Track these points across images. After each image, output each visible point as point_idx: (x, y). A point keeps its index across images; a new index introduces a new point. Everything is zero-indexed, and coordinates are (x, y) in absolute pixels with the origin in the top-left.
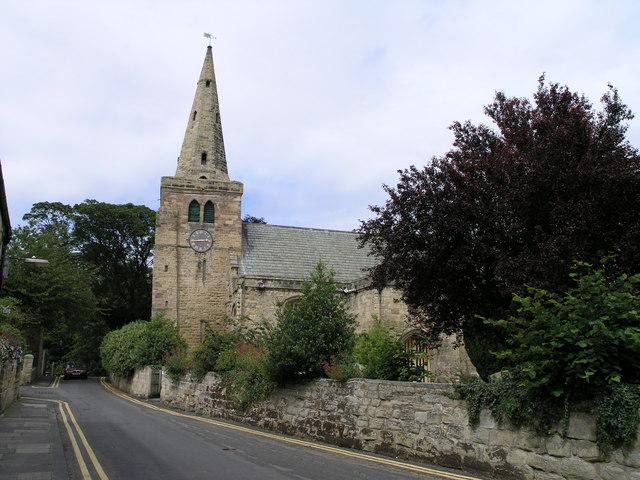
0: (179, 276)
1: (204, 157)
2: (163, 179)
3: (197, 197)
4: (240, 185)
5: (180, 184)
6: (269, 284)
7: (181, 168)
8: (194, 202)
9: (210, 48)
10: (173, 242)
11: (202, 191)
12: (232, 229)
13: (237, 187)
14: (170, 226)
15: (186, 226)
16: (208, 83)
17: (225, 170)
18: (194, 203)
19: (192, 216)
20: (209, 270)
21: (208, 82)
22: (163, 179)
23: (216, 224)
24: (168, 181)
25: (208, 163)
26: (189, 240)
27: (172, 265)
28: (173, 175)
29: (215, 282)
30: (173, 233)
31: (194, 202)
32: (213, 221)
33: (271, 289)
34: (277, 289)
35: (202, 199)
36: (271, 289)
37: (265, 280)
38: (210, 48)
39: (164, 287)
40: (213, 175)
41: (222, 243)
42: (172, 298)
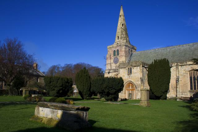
3: (115, 49)
6: (111, 71)
8: (114, 50)
10: (110, 62)
18: (115, 51)
19: (114, 55)
30: (110, 60)
31: (114, 50)
32: (119, 55)
33: (111, 72)
34: (113, 72)
35: (116, 49)
36: (111, 72)
37: (110, 70)
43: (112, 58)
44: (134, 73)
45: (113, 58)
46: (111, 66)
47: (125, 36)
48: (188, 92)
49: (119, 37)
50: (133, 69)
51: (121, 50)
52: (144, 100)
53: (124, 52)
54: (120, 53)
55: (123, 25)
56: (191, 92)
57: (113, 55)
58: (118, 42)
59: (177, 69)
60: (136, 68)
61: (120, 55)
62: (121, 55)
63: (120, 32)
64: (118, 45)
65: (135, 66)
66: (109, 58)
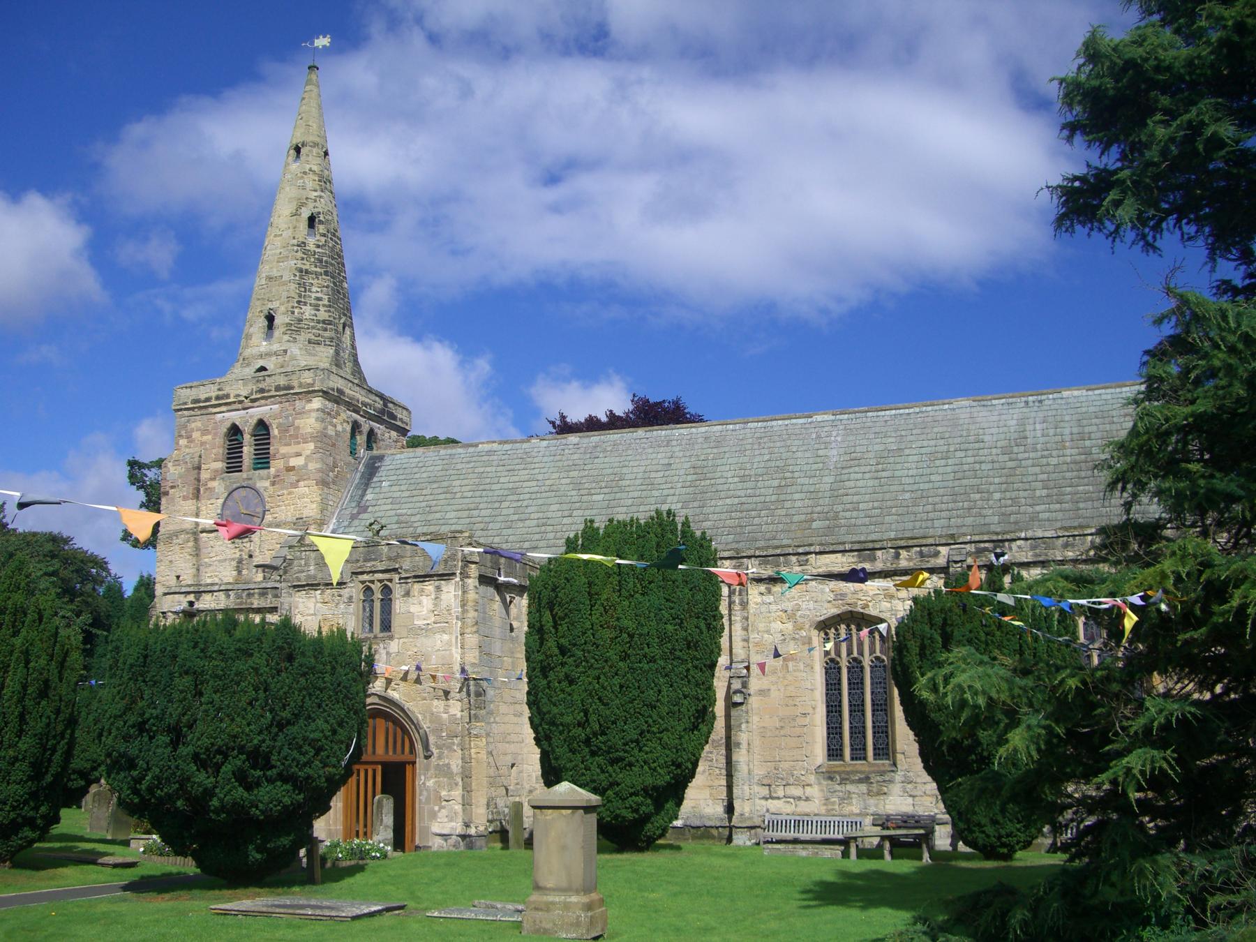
3: (236, 417)
5: (203, 397)
15: (219, 486)
18: (235, 431)
19: (233, 461)
23: (272, 470)
25: (277, 333)
30: (190, 505)
35: (246, 419)
40: (280, 359)
43: (211, 490)
44: (416, 632)
45: (219, 486)
46: (197, 553)
47: (323, 314)
48: (812, 778)
49: (277, 322)
50: (407, 594)
51: (284, 429)
52: (564, 884)
53: (311, 446)
54: (284, 450)
55: (312, 221)
56: (831, 779)
57: (220, 465)
58: (270, 364)
59: (737, 607)
60: (430, 587)
61: (276, 465)
62: (290, 469)
63: (287, 276)
64: (269, 383)
65: (423, 578)
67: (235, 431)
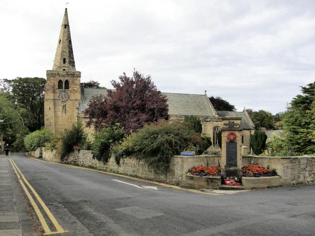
0: (55, 112)
1: (64, 61)
2: (47, 71)
3: (62, 79)
4: (80, 72)
7: (55, 65)
9: (66, 9)
11: (64, 76)
12: (76, 91)
13: (78, 73)
14: (50, 91)
15: (57, 91)
16: (65, 27)
17: (74, 66)
19: (60, 86)
20: (67, 109)
21: (66, 26)
22: (47, 71)
23: (70, 90)
24: (49, 72)
26: (59, 97)
27: (52, 107)
28: (51, 69)
29: (70, 114)
30: (52, 94)
35: (64, 79)
38: (66, 9)
39: (49, 116)
41: (72, 97)
42: (53, 121)
53: (78, 86)
58: (66, 69)
66: (50, 91)
67: (60, 82)
